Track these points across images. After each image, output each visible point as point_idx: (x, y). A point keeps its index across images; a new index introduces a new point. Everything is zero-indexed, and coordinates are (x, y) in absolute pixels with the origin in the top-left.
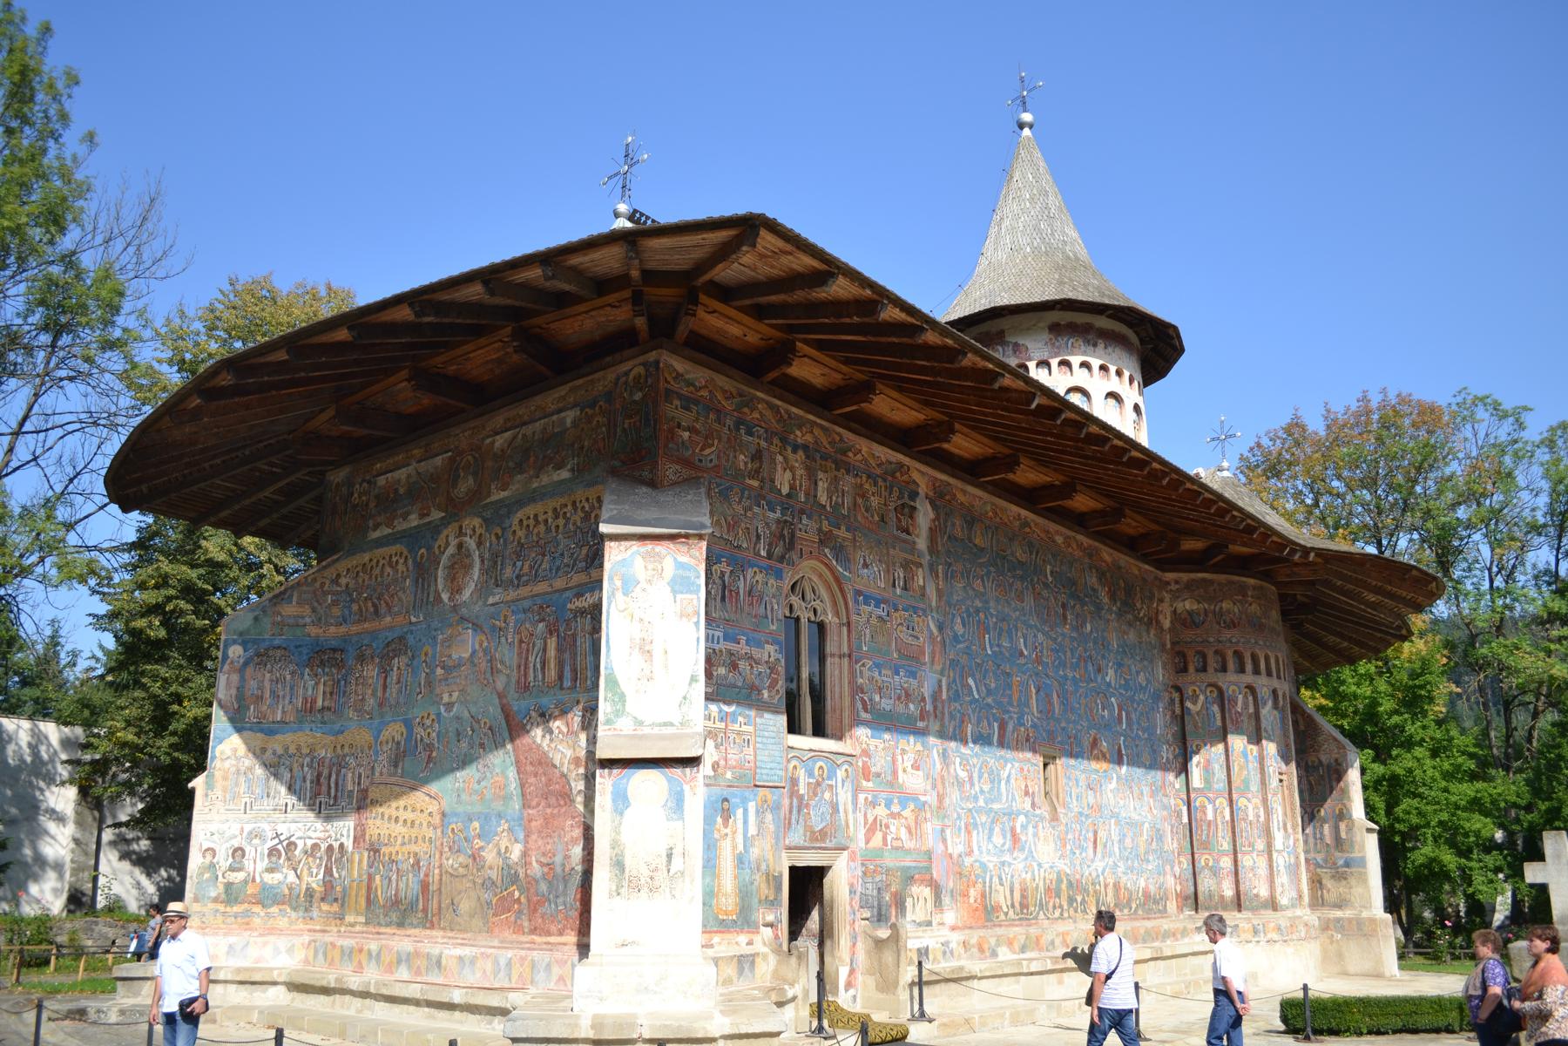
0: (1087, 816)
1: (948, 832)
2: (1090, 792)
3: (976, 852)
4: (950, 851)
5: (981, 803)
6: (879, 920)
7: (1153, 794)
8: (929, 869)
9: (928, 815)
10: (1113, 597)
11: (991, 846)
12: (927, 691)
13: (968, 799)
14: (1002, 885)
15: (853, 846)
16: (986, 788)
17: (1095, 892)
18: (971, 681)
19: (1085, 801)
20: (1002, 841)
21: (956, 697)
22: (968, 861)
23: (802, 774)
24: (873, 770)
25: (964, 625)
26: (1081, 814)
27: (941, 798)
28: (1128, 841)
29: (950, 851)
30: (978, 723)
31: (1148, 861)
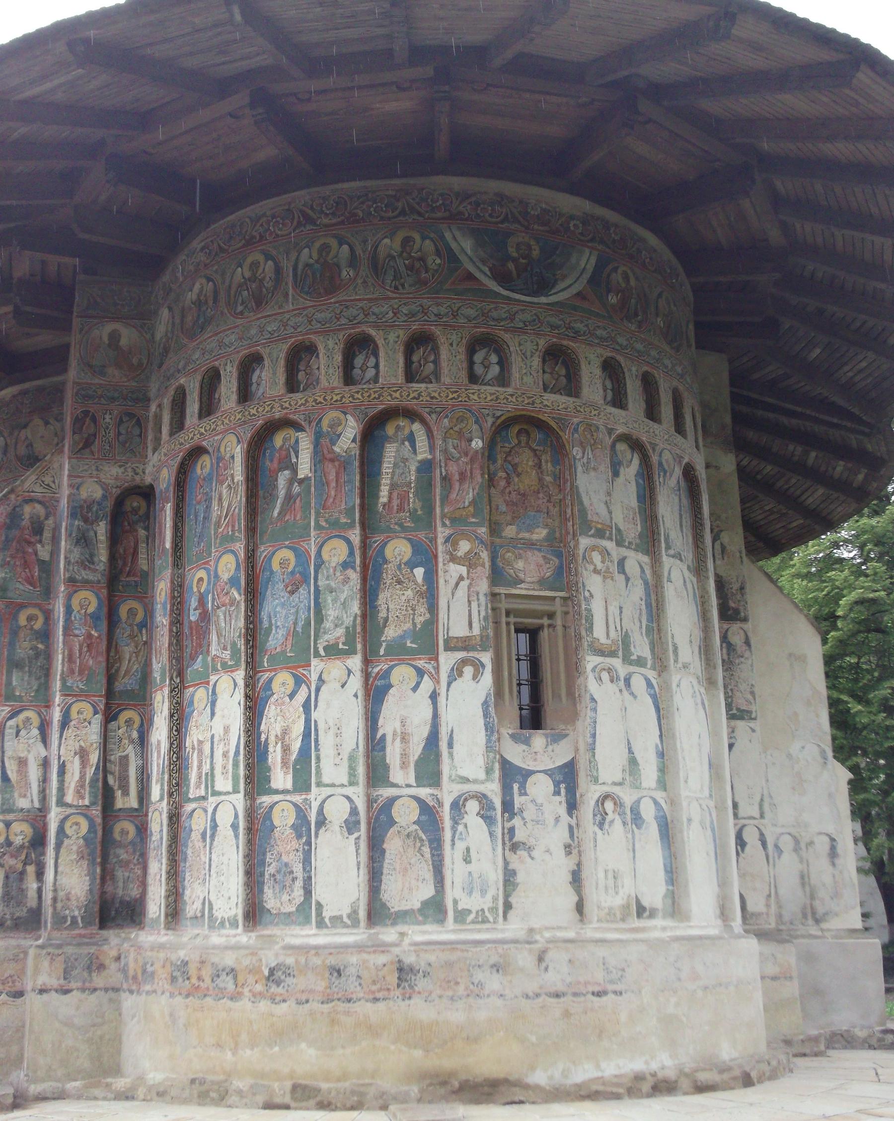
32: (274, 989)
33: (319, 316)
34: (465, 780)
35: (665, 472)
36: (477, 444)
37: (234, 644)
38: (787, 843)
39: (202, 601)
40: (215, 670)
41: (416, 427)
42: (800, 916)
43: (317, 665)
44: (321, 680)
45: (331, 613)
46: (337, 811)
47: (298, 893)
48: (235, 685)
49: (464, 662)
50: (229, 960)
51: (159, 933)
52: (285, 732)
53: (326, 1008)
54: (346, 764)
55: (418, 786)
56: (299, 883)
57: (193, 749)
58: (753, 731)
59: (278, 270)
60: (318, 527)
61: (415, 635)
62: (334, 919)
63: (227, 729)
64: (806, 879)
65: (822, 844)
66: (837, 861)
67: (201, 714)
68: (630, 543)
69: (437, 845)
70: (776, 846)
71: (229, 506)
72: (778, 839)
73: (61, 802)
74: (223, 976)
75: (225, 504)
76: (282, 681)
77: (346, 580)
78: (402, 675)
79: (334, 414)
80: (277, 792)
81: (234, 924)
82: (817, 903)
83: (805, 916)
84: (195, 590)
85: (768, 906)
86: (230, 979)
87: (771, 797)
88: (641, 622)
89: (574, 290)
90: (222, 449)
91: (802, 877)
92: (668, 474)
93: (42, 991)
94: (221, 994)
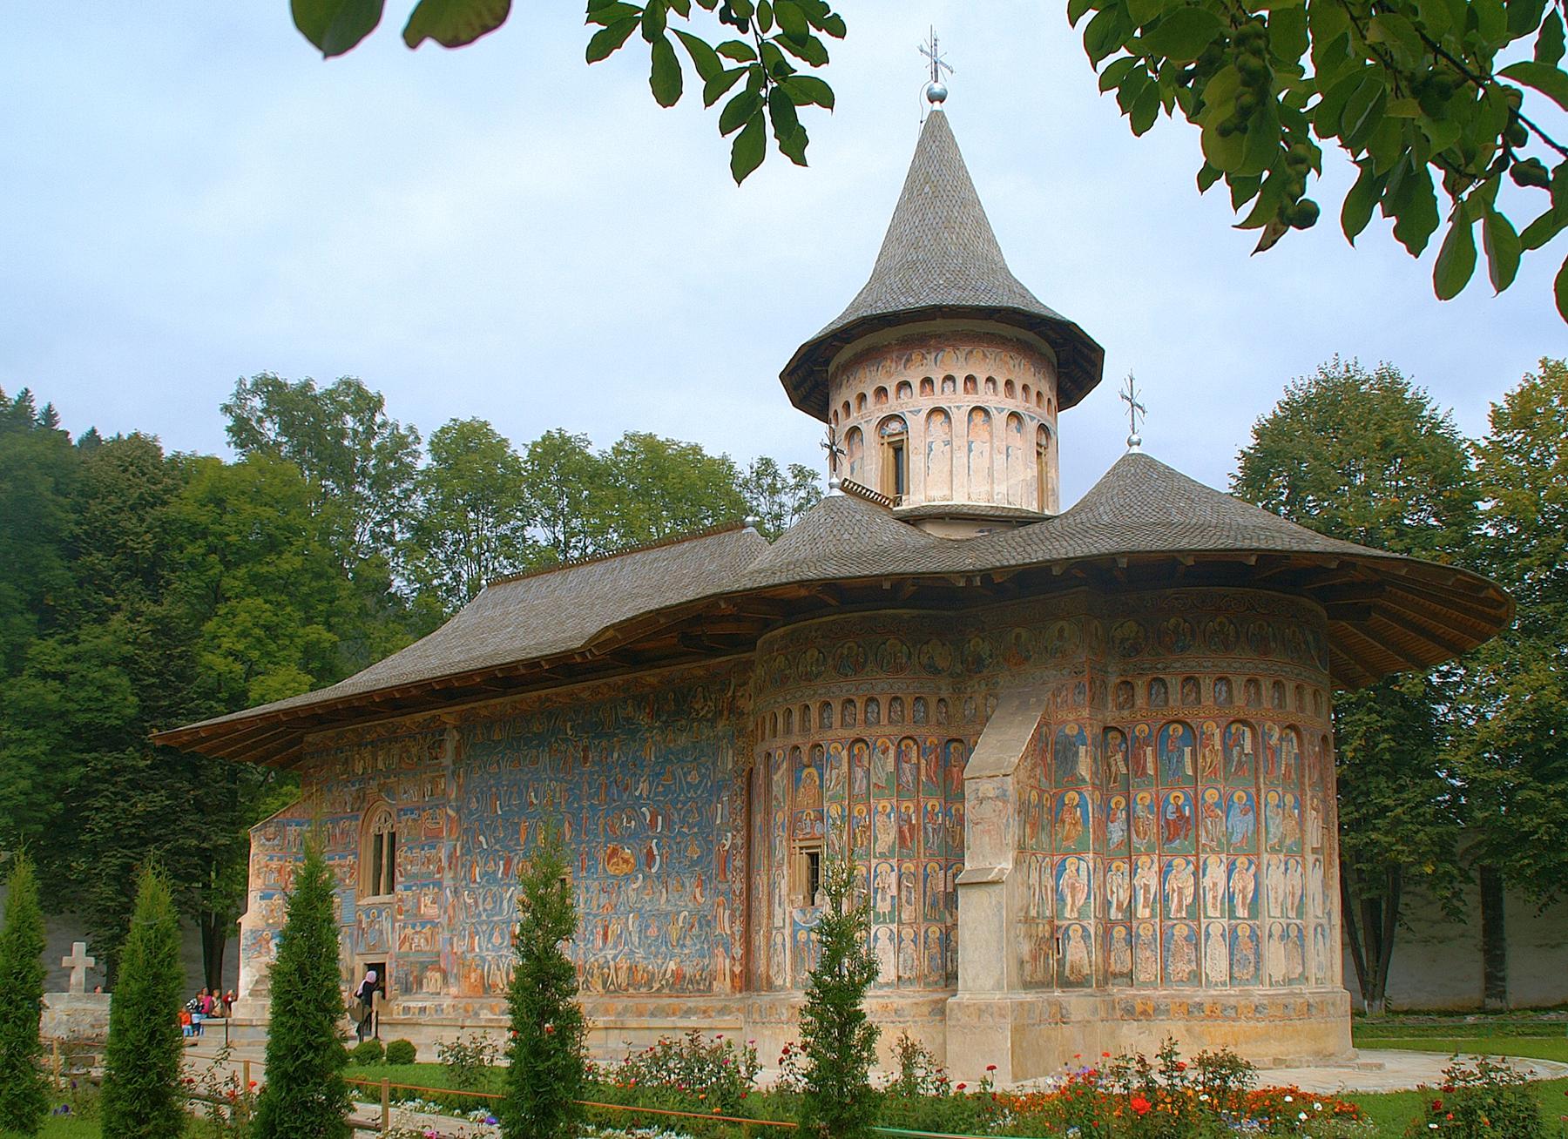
0: (595, 916)
1: (455, 939)
2: (602, 895)
3: (477, 950)
4: (455, 950)
5: (484, 917)
6: (406, 991)
7: (701, 884)
8: (438, 962)
9: (441, 930)
10: (655, 715)
11: (490, 945)
12: (443, 855)
13: (472, 916)
14: (499, 970)
15: (391, 951)
16: (488, 907)
17: (603, 974)
18: (482, 838)
19: (595, 903)
20: (500, 941)
21: (467, 851)
22: (469, 956)
23: (364, 917)
24: (404, 909)
25: (478, 802)
26: (588, 914)
27: (450, 919)
28: (653, 932)
29: (455, 950)
30: (485, 864)
31: (684, 946)
32: (1258, 1015)
33: (1261, 666)
34: (1318, 917)
36: (1317, 749)
37: (1219, 840)
39: (1179, 809)
40: (1204, 851)
41: (1293, 734)
43: (1265, 857)
44: (1269, 865)
45: (1272, 830)
46: (1277, 930)
47: (1252, 969)
48: (1221, 861)
49: (1317, 860)
50: (1232, 1001)
51: (1156, 989)
52: (1245, 888)
53: (1282, 1023)
54: (1279, 909)
55: (1297, 918)
56: (1252, 965)
57: (1174, 891)
59: (1237, 632)
60: (1265, 784)
61: (1296, 844)
62: (1276, 982)
63: (1215, 884)
67: (1178, 872)
69: (1302, 946)
71: (1212, 762)
73: (1095, 916)
74: (1229, 1010)
75: (1209, 760)
76: (1241, 861)
77: (1278, 814)
78: (1292, 862)
79: (1270, 723)
80: (1239, 918)
81: (1224, 984)
84: (1172, 801)
86: (1233, 1011)
90: (1205, 727)
93: (1102, 1021)
94: (1227, 1018)
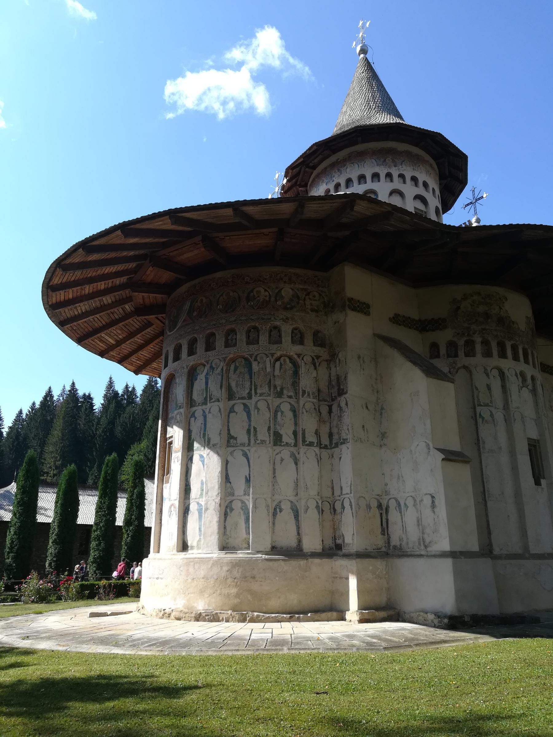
35: (213, 369)
38: (410, 502)
42: (417, 544)
58: (348, 448)
64: (420, 522)
65: (427, 501)
66: (435, 510)
68: (199, 404)
70: (405, 504)
72: (406, 500)
82: (426, 536)
83: (420, 544)
85: (353, 540)
87: (402, 477)
88: (200, 433)
89: (183, 320)
91: (418, 521)
92: (215, 369)
